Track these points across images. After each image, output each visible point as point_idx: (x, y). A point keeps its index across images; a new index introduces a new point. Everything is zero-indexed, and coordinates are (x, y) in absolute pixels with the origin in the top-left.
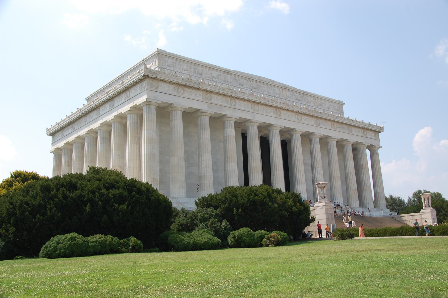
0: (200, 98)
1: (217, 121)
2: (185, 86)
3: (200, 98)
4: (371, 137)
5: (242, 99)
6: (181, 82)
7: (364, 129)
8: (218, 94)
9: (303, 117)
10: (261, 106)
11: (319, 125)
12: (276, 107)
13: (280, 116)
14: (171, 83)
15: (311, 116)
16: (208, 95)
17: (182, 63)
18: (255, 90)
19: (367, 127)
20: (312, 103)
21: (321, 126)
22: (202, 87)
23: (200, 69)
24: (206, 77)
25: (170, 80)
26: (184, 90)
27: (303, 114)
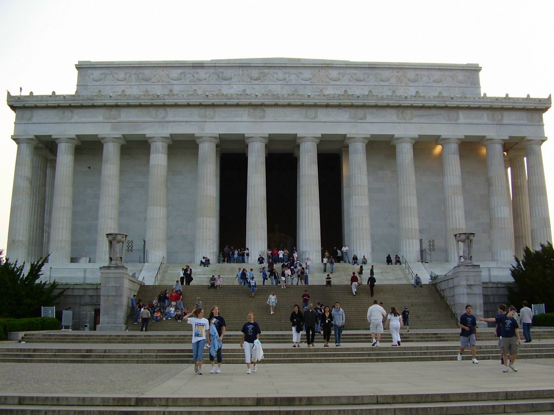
0: (100, 119)
2: (70, 107)
3: (100, 119)
4: (516, 122)
5: (176, 106)
6: (62, 103)
7: (491, 108)
8: (128, 106)
11: (365, 118)
12: (250, 105)
13: (264, 117)
14: (47, 107)
15: (340, 106)
16: (114, 112)
17: (116, 71)
18: (257, 82)
20: (393, 81)
21: (369, 118)
23: (147, 72)
24: (159, 81)
25: (44, 104)
27: (315, 106)
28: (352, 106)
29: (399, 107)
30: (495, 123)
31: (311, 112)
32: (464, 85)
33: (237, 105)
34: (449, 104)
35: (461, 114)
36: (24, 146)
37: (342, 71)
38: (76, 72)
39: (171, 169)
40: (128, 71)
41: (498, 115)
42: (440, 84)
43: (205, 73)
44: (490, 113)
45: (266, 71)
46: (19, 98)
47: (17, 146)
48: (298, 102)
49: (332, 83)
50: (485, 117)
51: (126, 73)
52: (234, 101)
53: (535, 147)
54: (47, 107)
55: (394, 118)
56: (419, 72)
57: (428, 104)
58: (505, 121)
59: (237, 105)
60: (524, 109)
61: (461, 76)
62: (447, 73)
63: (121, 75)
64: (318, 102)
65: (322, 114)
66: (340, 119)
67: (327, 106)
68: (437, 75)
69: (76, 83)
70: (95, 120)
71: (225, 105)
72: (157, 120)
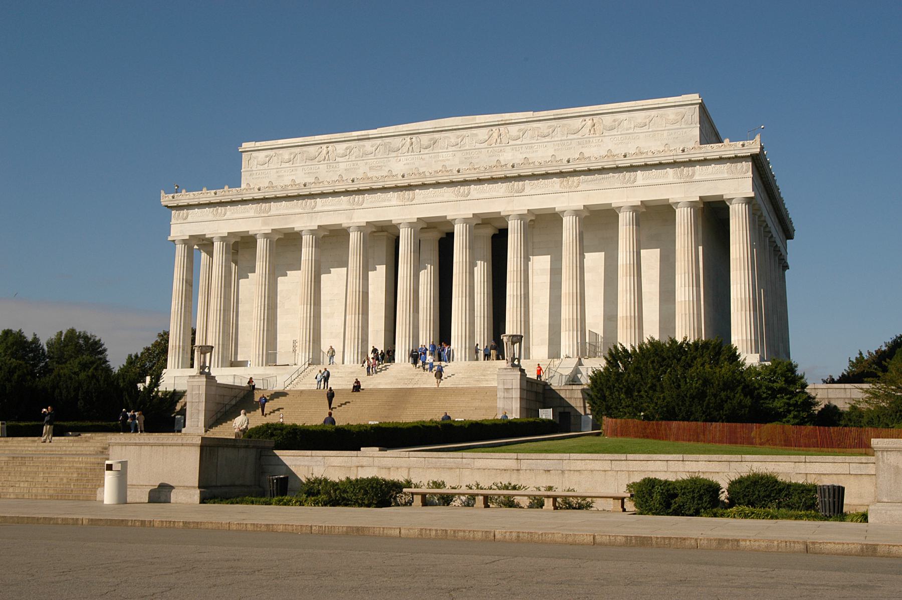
0: (252, 214)
13: (413, 199)
18: (427, 151)
20: (586, 130)
21: (528, 190)
29: (561, 173)
30: (682, 180)
42: (645, 129)
43: (372, 146)
45: (436, 136)
49: (511, 143)
51: (291, 154)
58: (697, 177)
66: (495, 194)
70: (247, 215)
71: (372, 191)
72: (306, 211)
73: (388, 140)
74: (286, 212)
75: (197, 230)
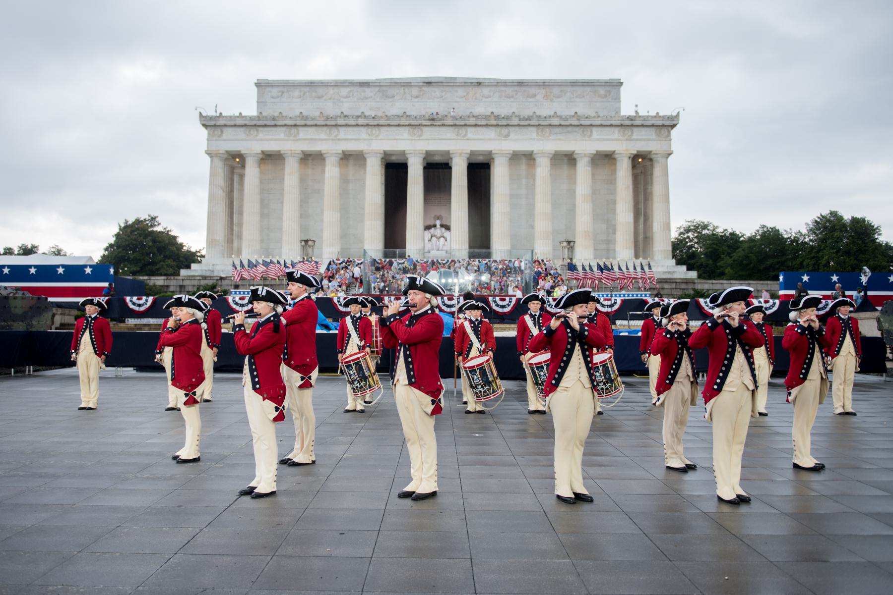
1: (311, 159)
3: (282, 136)
5: (347, 125)
6: (248, 123)
7: (622, 125)
8: (305, 125)
9: (470, 129)
10: (383, 129)
11: (508, 135)
13: (420, 136)
16: (294, 130)
18: (416, 100)
19: (628, 123)
21: (512, 136)
22: (278, 123)
23: (321, 91)
25: (232, 123)
26: (257, 131)
27: (466, 125)
28: (497, 125)
31: (462, 131)
32: (604, 100)
33: (399, 125)
34: (583, 122)
35: (595, 130)
36: (215, 159)
37: (493, 88)
38: (256, 89)
39: (344, 181)
40: (304, 89)
41: (628, 132)
44: (622, 130)
45: (425, 89)
46: (211, 118)
47: (208, 159)
48: (451, 122)
49: (484, 100)
50: (616, 133)
52: (396, 122)
53: (662, 160)
54: (235, 126)
55: (534, 135)
56: (564, 88)
57: (563, 123)
58: (634, 137)
59: (399, 125)
60: (653, 126)
61: (602, 91)
62: (588, 89)
63: (297, 93)
64: (467, 122)
65: (471, 132)
67: (476, 125)
68: (580, 90)
69: (256, 99)
71: (389, 125)
73: (384, 88)
74: (313, 137)
75: (233, 147)
